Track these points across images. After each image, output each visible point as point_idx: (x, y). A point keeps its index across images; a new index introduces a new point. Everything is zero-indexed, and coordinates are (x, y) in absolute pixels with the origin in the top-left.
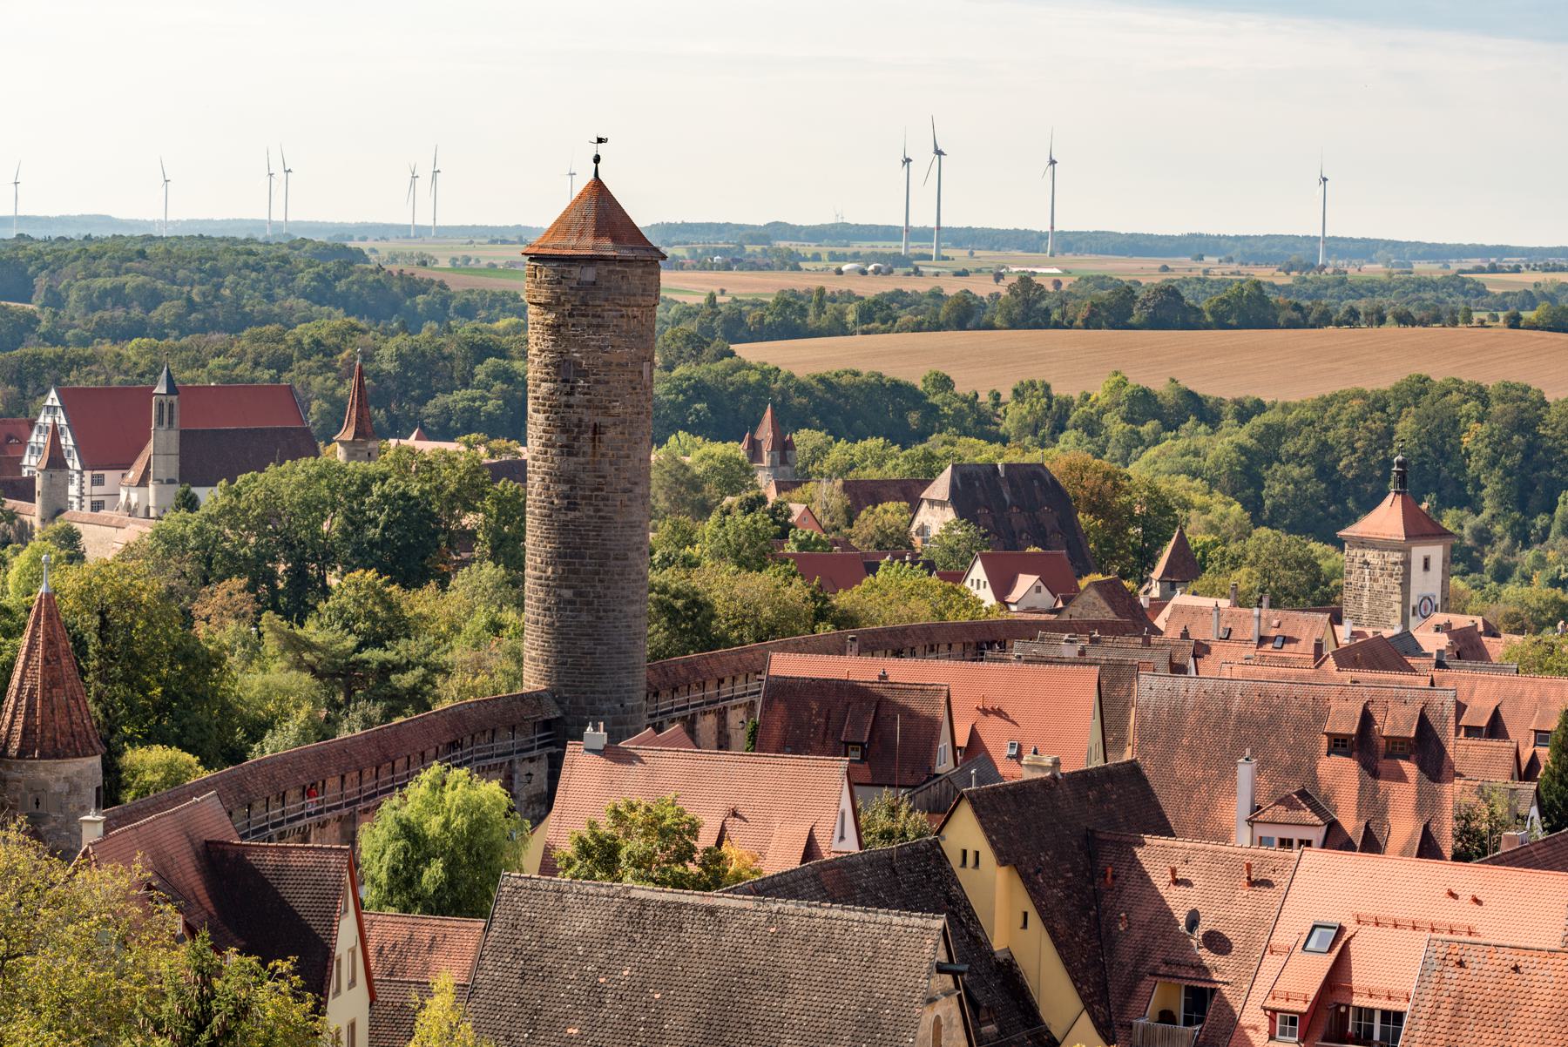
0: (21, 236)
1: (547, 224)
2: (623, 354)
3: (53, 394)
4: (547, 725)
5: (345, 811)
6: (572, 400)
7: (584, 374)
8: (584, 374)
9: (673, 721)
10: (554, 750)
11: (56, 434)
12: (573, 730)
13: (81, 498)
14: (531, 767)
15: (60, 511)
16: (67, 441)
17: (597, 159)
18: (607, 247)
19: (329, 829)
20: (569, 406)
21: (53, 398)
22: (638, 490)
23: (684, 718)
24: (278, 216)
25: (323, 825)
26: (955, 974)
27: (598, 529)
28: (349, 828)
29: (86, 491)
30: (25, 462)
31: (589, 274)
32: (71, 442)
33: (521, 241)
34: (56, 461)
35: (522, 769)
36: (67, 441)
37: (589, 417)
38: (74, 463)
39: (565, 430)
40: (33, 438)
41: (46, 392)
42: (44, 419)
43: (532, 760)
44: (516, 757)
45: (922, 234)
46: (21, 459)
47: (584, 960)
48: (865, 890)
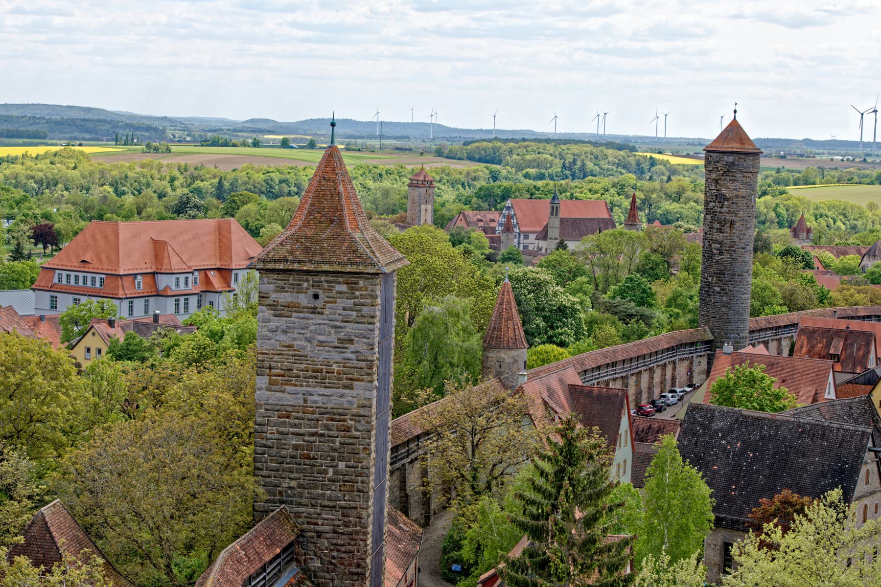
1: (714, 137)
2: (743, 192)
3: (509, 202)
4: (707, 342)
5: (624, 374)
6: (722, 210)
7: (727, 199)
8: (727, 199)
9: (759, 343)
10: (710, 352)
12: (718, 345)
14: (700, 359)
17: (735, 112)
18: (736, 146)
19: (617, 381)
20: (721, 213)
22: (748, 247)
23: (763, 342)
24: (601, 132)
25: (615, 380)
26: (876, 452)
27: (731, 263)
28: (625, 381)
31: (731, 159)
33: (700, 144)
35: (696, 361)
37: (729, 217)
39: (720, 223)
43: (701, 356)
44: (695, 355)
45: (868, 145)
47: (722, 438)
48: (839, 415)
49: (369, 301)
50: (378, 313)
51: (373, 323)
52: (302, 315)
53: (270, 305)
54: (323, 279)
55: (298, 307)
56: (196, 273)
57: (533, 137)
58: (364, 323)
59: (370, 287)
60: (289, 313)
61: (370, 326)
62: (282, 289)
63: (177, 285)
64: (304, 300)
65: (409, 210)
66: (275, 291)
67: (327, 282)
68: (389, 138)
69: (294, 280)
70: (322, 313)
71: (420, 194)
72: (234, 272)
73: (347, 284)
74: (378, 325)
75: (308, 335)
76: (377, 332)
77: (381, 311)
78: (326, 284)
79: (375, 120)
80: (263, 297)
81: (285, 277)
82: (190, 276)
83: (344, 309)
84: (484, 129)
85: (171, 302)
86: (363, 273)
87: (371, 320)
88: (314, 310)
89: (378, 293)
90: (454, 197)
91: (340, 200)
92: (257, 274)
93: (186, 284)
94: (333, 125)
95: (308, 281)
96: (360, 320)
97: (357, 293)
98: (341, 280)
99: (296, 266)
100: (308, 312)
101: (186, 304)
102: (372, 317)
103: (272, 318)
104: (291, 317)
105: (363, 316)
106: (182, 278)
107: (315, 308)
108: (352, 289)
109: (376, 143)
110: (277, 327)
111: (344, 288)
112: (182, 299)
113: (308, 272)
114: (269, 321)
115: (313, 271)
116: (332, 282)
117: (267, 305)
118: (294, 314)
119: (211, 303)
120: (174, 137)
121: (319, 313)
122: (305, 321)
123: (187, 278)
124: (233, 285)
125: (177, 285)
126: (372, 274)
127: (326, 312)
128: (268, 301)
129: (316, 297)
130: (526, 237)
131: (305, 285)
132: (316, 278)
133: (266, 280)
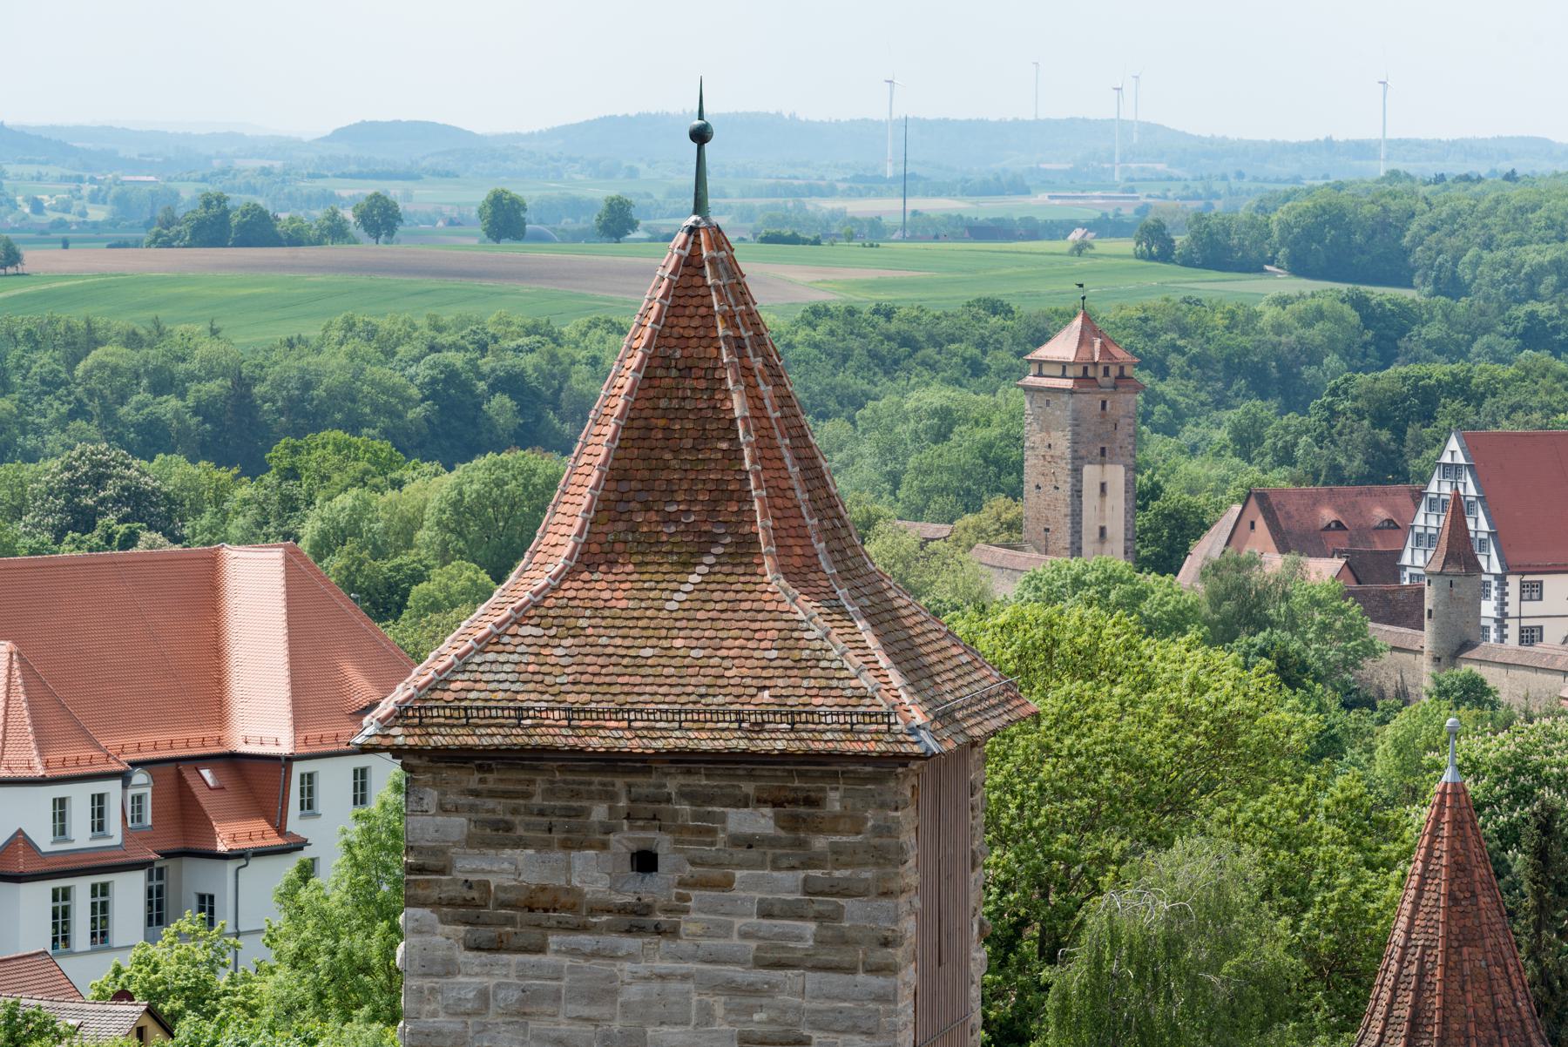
0: (1394, 175)
3: (1453, 444)
11: (1459, 509)
13: (1501, 623)
15: (1466, 645)
16: (1479, 524)
21: (1454, 452)
29: (1512, 610)
30: (1406, 559)
32: (1484, 525)
34: (1461, 554)
36: (1479, 524)
38: (1491, 563)
40: (1420, 520)
41: (1439, 442)
42: (1438, 487)
46: (1399, 554)
49: (868, 874)
50: (909, 925)
51: (888, 969)
52: (585, 940)
53: (451, 903)
54: (671, 786)
55: (572, 908)
56: (140, 777)
57: (1545, 167)
58: (851, 970)
59: (872, 818)
60: (534, 936)
61: (877, 982)
62: (497, 834)
63: (61, 830)
64: (592, 875)
65: (1028, 488)
66: (472, 842)
67: (689, 796)
68: (939, 191)
69: (550, 793)
70: (672, 932)
71: (1077, 422)
72: (298, 769)
73: (776, 804)
74: (909, 974)
75: (616, 1026)
76: (905, 1004)
77: (921, 917)
78: (686, 808)
79: (879, 113)
80: (420, 869)
81: (511, 779)
82: (113, 788)
83: (766, 912)
84: (1340, 136)
85: (36, 899)
86: (842, 757)
87: (880, 955)
88: (637, 920)
89: (908, 838)
90: (1221, 435)
91: (735, 454)
92: (386, 773)
93: (99, 826)
94: (700, 136)
95: (610, 796)
96: (835, 958)
97: (820, 843)
98: (748, 788)
99: (563, 739)
100: (611, 929)
101: (101, 911)
102: (886, 943)
103: (463, 956)
104: (541, 949)
105: (843, 940)
106: (80, 797)
107: (648, 910)
108: (792, 823)
109: (887, 207)
110: (484, 996)
111: (761, 821)
112: (81, 888)
113: (613, 761)
114: (449, 969)
115: (630, 756)
116: (710, 799)
117: (437, 904)
118: (554, 940)
119: (206, 903)
120: (37, 207)
121: (658, 930)
122: (597, 965)
123: (99, 799)
124: (295, 823)
125: (61, 830)
126: (882, 758)
127: (690, 924)
128: (448, 886)
129: (645, 862)
130: (1532, 591)
131: (599, 812)
132: (644, 784)
133: (431, 797)
